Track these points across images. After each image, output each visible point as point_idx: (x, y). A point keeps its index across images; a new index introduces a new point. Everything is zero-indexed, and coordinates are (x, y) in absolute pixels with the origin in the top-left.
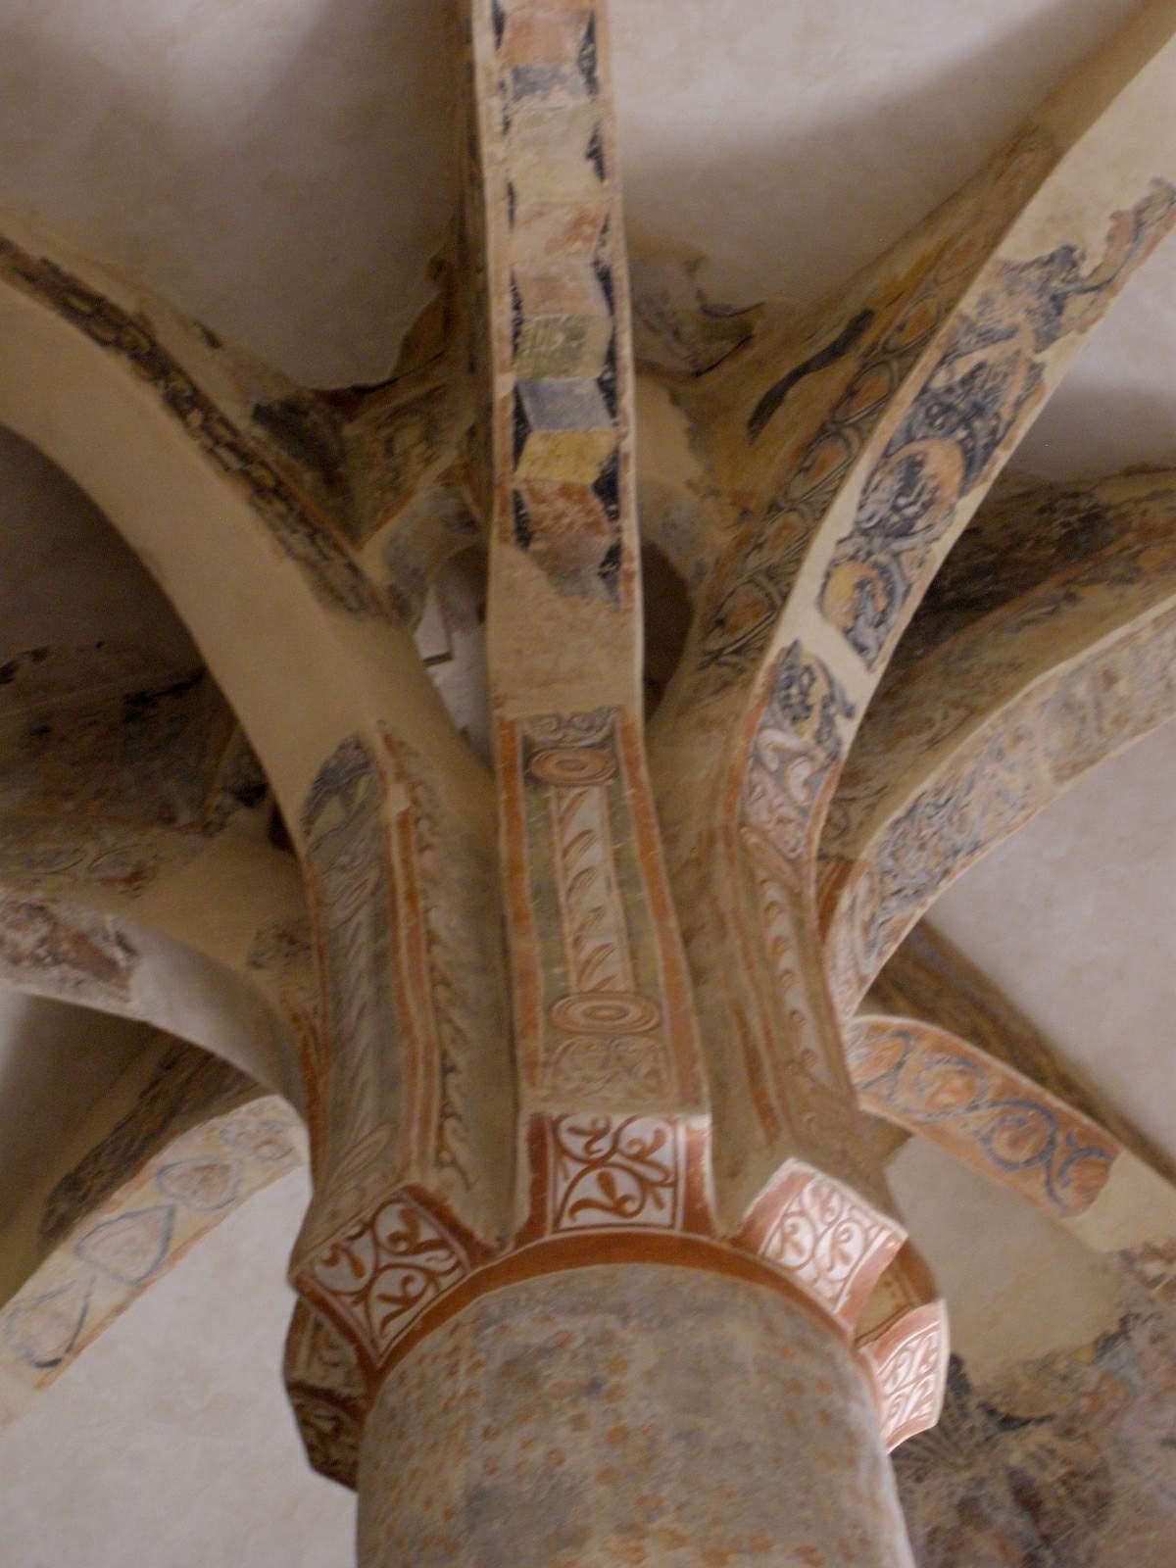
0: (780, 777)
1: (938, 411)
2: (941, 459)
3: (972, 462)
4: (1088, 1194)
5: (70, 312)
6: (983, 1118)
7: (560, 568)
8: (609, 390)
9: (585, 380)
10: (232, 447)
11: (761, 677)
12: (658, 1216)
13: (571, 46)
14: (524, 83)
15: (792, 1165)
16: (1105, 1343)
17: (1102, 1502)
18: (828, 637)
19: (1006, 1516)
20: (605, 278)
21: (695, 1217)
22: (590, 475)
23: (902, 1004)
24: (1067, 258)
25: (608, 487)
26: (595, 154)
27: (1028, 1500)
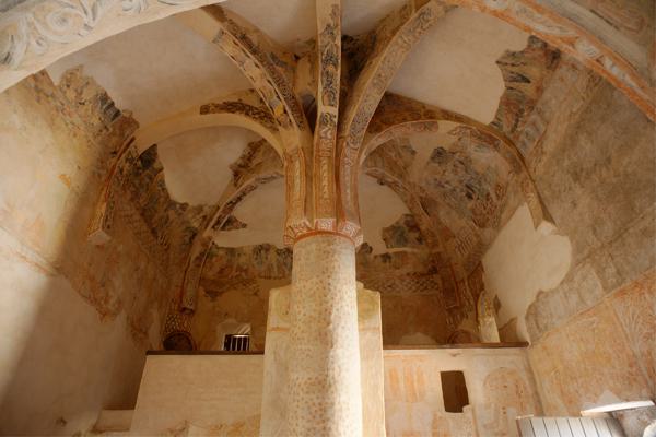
0: (326, 138)
1: (326, 62)
2: (331, 68)
3: (335, 65)
4: (437, 127)
5: (229, 111)
6: (412, 129)
7: (285, 127)
8: (278, 97)
9: (275, 98)
10: (259, 113)
11: (318, 122)
12: (305, 231)
13: (242, 53)
14: (242, 63)
15: (315, 221)
16: (460, 139)
17: (471, 161)
18: (327, 109)
19: (460, 165)
20: (269, 81)
21: (309, 229)
22: (282, 111)
23: (384, 126)
24: (329, 26)
25: (285, 112)
26: (257, 65)
27: (461, 162)
